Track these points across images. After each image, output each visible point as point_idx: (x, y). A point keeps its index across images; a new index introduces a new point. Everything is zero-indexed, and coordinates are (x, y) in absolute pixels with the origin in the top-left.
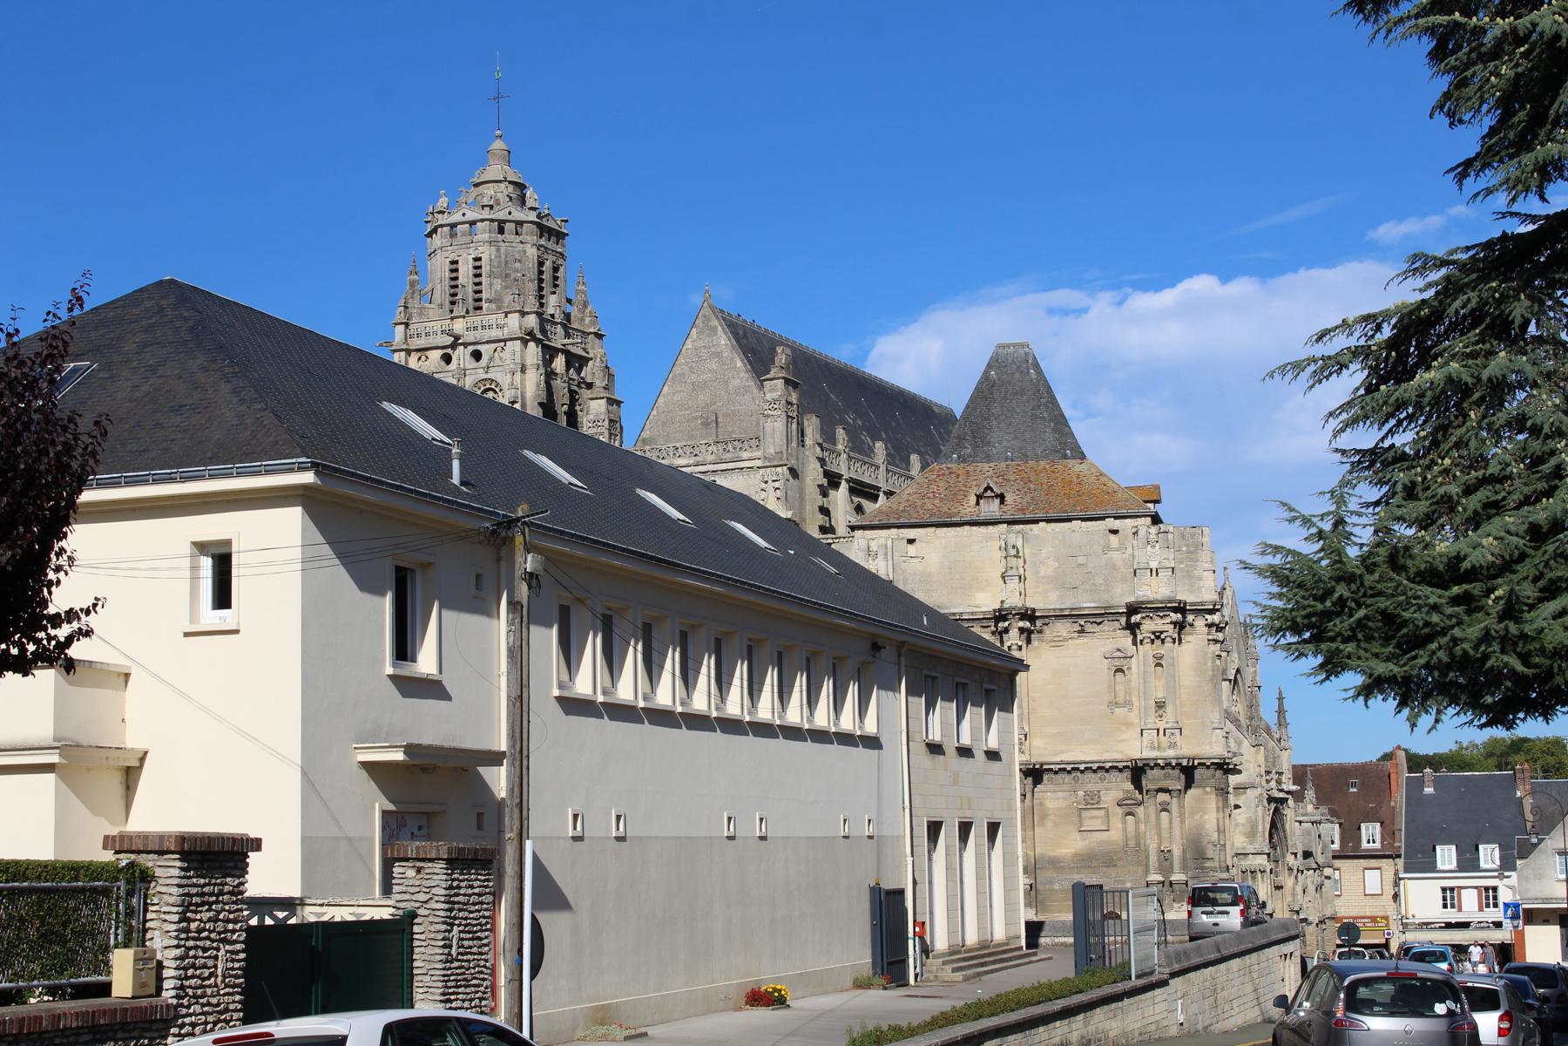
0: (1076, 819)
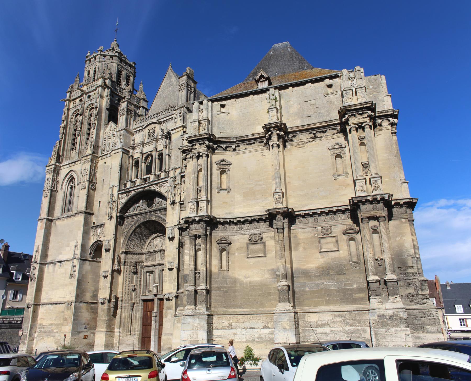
0: (317, 244)
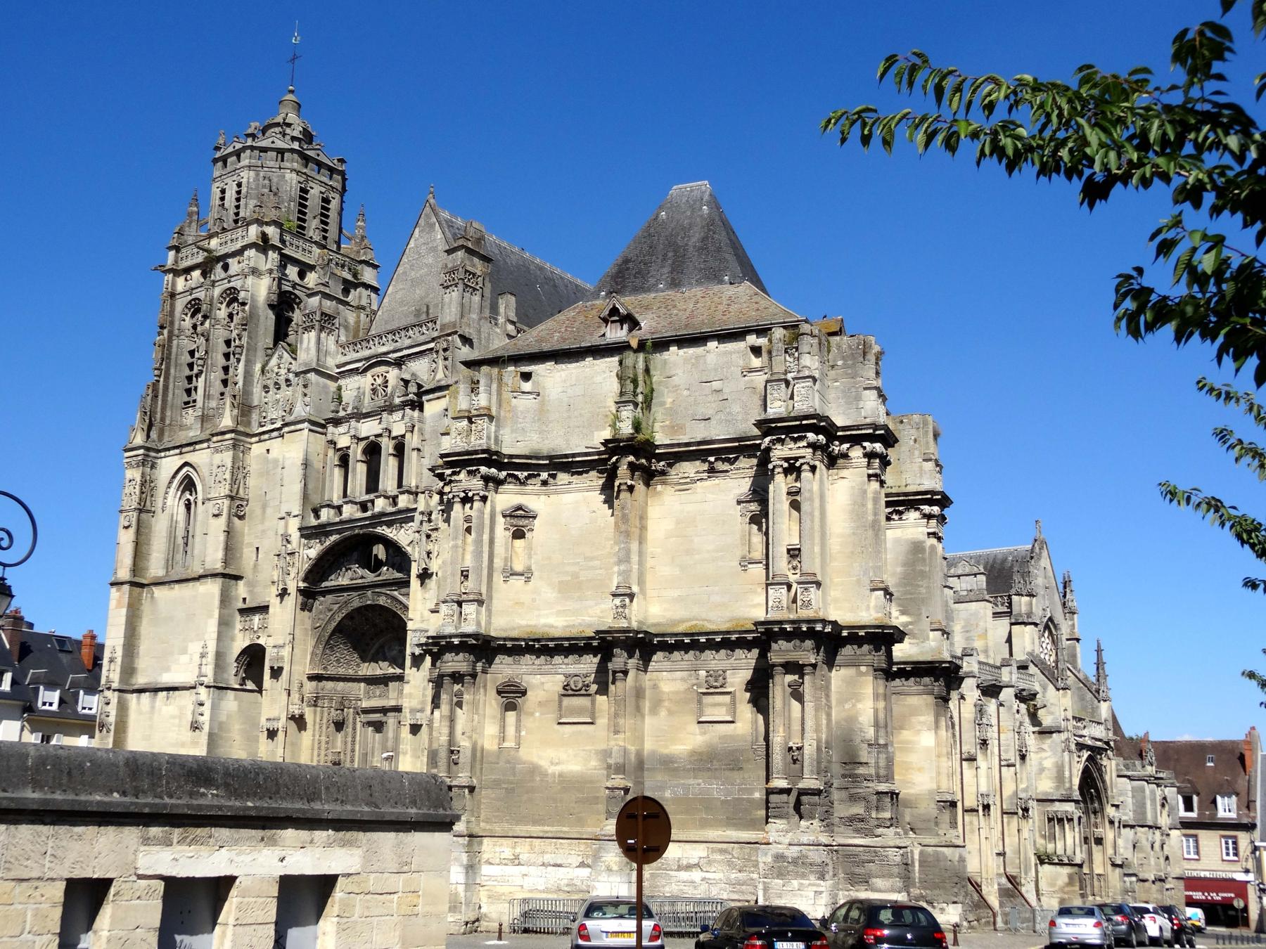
0: (694, 706)
